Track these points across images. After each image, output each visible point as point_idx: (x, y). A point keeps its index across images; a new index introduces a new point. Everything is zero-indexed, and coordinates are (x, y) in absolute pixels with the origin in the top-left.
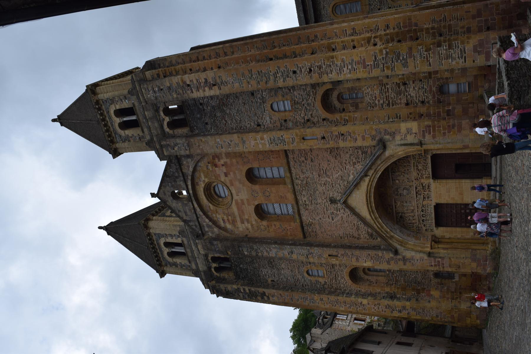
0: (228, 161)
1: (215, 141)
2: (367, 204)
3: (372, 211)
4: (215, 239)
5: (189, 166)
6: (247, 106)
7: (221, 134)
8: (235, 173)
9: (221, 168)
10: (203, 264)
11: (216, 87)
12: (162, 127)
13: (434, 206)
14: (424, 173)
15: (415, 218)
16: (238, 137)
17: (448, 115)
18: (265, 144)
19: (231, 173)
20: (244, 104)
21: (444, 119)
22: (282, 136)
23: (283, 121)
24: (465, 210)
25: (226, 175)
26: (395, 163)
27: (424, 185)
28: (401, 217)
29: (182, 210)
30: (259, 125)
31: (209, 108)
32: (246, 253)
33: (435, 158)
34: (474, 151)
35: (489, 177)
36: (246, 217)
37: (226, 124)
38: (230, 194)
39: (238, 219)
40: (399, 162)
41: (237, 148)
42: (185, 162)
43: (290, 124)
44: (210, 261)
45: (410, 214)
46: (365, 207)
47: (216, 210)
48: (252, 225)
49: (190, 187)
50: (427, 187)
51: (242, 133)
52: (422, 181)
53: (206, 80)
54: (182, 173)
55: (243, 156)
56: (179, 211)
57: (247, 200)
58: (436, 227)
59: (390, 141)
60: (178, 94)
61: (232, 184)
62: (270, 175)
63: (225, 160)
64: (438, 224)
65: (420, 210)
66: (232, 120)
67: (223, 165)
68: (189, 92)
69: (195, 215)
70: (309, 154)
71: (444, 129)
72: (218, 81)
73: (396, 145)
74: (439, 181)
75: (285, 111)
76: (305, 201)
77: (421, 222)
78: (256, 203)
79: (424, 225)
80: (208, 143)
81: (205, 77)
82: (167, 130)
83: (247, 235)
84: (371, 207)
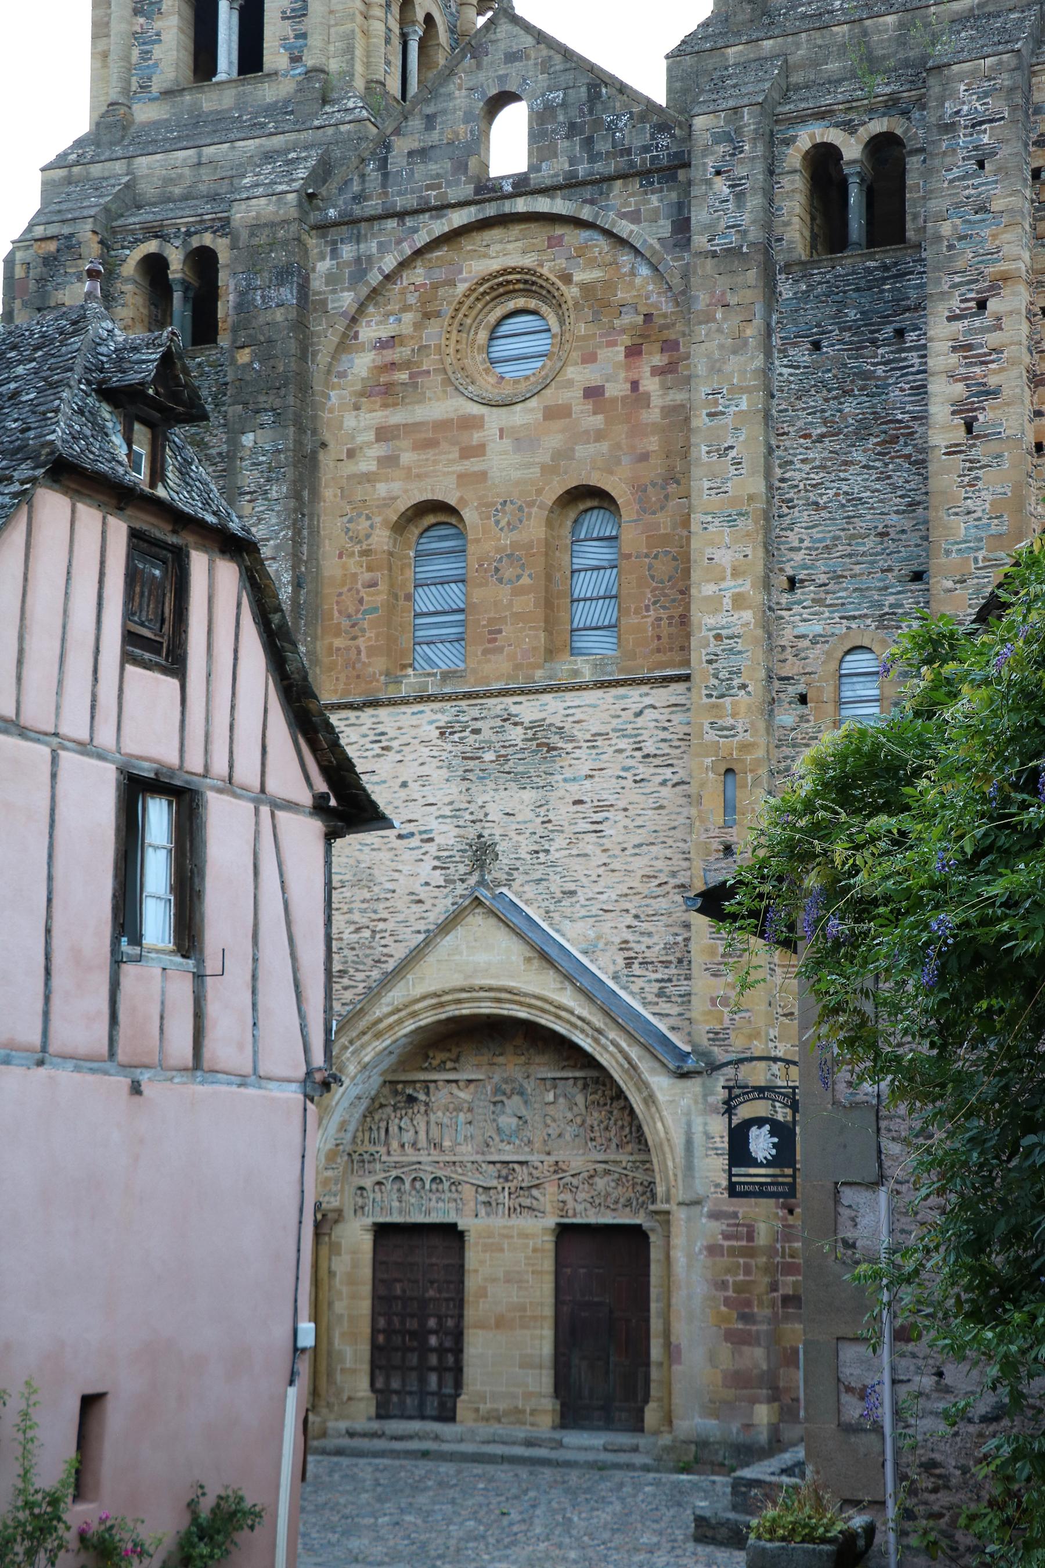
0: (653, 415)
1: (743, 390)
2: (471, 989)
3: (442, 1005)
4: (303, 289)
5: (638, 214)
6: (870, 543)
7: (767, 416)
8: (599, 436)
9: (622, 375)
10: (168, 181)
11: (960, 435)
12: (821, 115)
13: (455, 1225)
14: (581, 1196)
15: (409, 1150)
16: (751, 498)
17: (786, 1300)
18: (716, 611)
19: (600, 417)
20: (882, 535)
21: (774, 1287)
22: (744, 686)
23: (801, 688)
24: (435, 1332)
25: (593, 393)
26: (620, 1095)
27: (535, 1192)
28: (411, 1100)
29: (434, 137)
30: (793, 583)
31: (880, 371)
32: (248, 440)
33: (635, 1237)
34: (654, 1373)
35: (558, 1420)
36: (407, 458)
37: (805, 436)
38: (507, 390)
39: (397, 417)
40: (623, 1108)
41: (707, 484)
42: (654, 200)
43: (787, 717)
44: (195, 242)
45: (422, 1135)
46: (457, 980)
47: (438, 314)
48: (369, 478)
49: (543, 205)
50: (527, 1202)
51: (767, 516)
52: (551, 1189)
53: (993, 393)
54: (611, 178)
55: (672, 488)
56: (430, 121)
57: (483, 476)
58: (375, 1224)
59: (705, 1096)
60: (951, 247)
61: (552, 413)
62: (585, 585)
63: (657, 401)
64: (383, 1232)
65: (440, 1173)
66: (823, 467)
67: (635, 385)
68: (955, 303)
69: (410, 201)
70: (668, 772)
71: (739, 1288)
72: (980, 451)
73: (688, 1114)
74: (550, 1246)
75: (840, 703)
76: (476, 731)
77: (394, 1173)
78: (467, 514)
79: (379, 1183)
80: (735, 352)
81: (1006, 392)
82: (808, 136)
83: (324, 445)
84: (459, 1001)
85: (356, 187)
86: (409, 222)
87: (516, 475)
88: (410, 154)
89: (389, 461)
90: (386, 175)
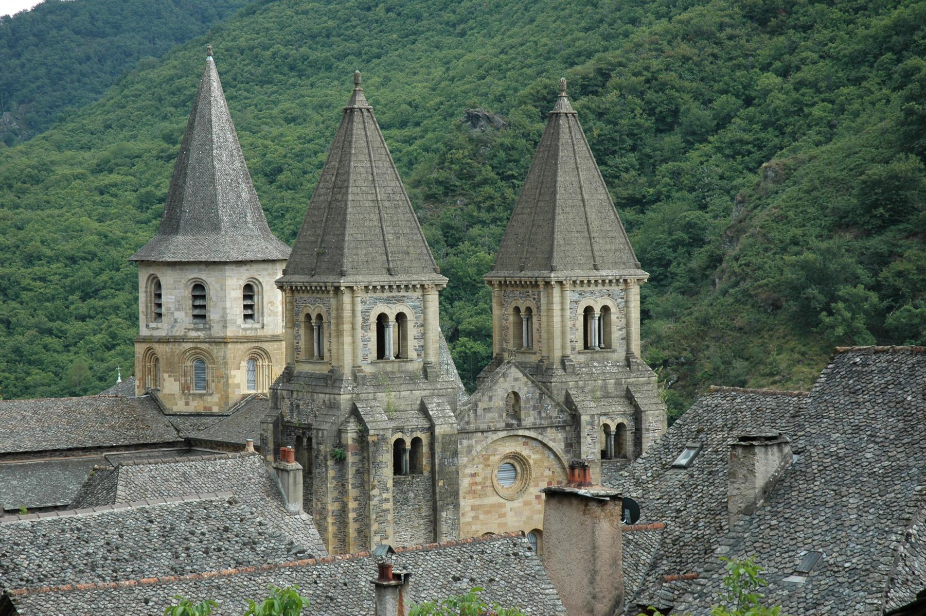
36: (481, 517)
39: (478, 502)
48: (469, 524)
49: (527, 433)
56: (490, 398)
57: (506, 524)
61: (527, 503)
85: (466, 419)
86: (485, 434)
87: (516, 524)
88: (484, 409)
89: (476, 518)
90: (476, 415)
